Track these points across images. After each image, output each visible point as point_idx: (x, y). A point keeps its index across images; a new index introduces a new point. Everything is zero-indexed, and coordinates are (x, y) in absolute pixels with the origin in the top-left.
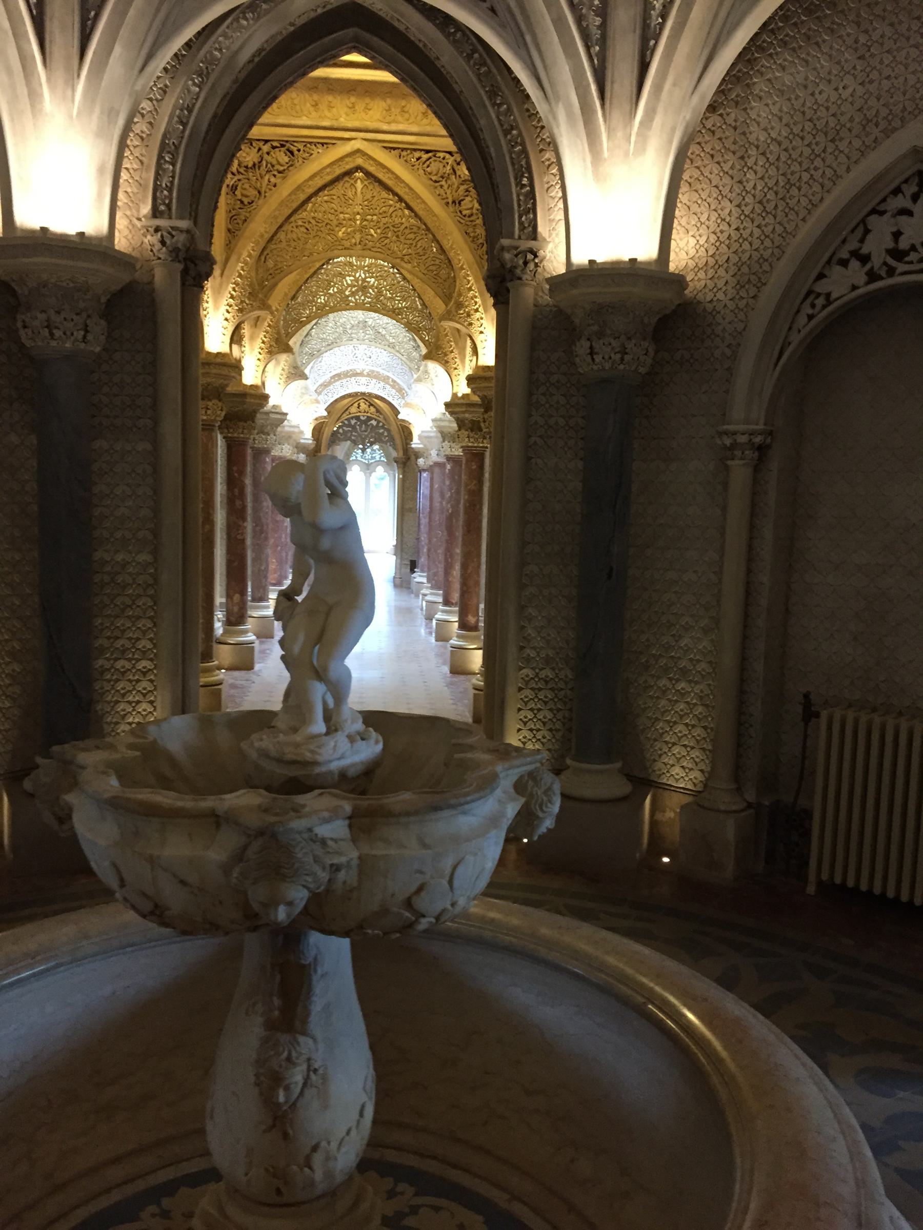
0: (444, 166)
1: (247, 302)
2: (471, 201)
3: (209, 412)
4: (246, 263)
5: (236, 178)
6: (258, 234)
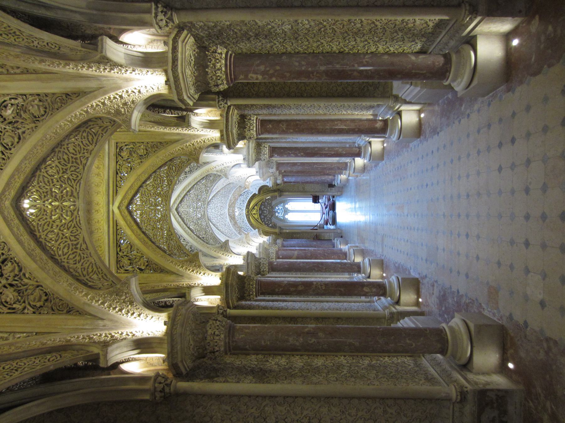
0: (7, 131)
1: (124, 297)
2: (33, 106)
3: (217, 333)
4: (92, 299)
5: (28, 307)
6: (69, 288)
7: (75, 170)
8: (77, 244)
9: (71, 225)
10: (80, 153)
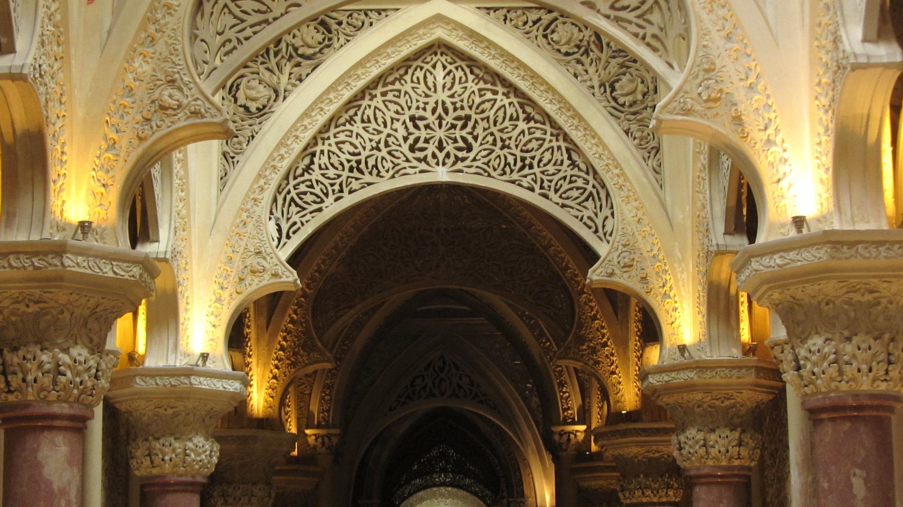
7: (509, 164)
8: (361, 171)
9: (398, 158)
10: (543, 172)
